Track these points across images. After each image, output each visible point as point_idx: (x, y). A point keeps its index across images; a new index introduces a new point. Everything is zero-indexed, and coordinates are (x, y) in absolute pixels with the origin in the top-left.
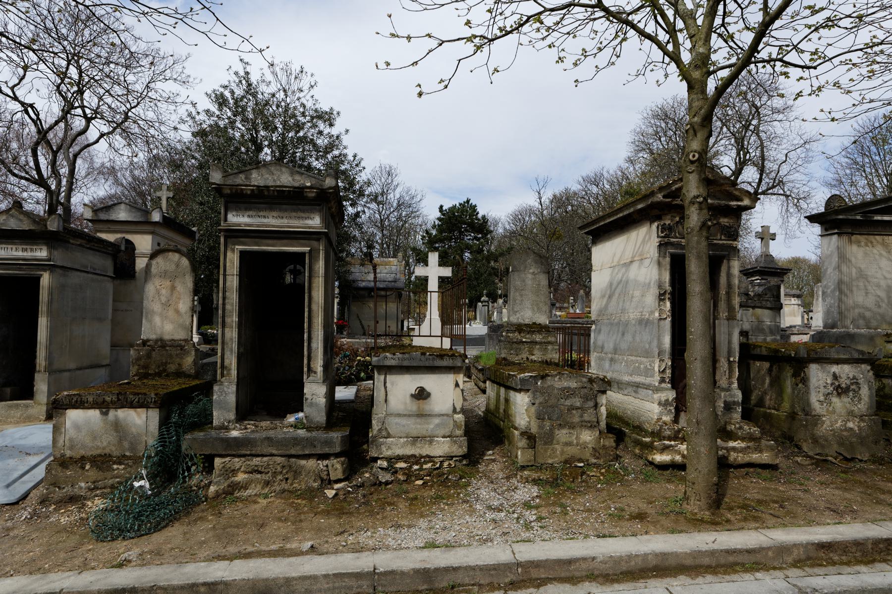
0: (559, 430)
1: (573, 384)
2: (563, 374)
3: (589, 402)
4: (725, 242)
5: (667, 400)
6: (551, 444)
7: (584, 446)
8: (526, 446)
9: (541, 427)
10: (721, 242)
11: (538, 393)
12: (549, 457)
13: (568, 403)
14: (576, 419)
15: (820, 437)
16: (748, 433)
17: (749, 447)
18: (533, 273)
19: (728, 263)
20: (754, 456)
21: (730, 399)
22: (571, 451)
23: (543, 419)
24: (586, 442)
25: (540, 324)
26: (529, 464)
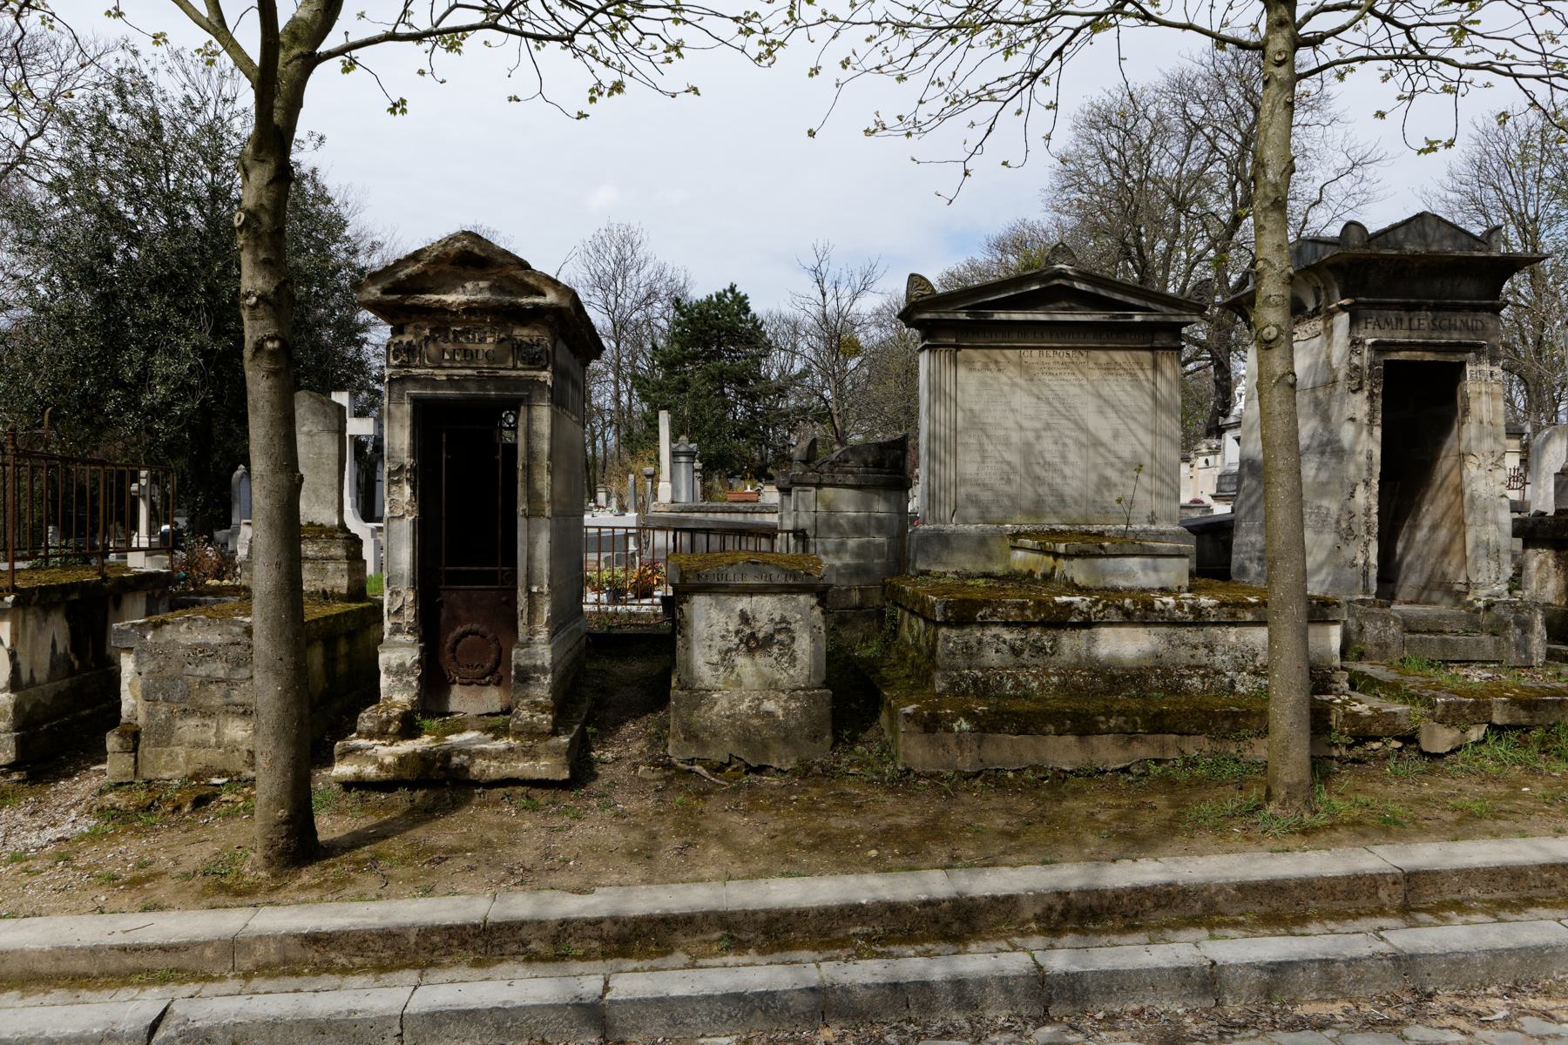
1: (214, 638)
3: (242, 670)
4: (522, 373)
5: (402, 665)
7: (234, 747)
8: (118, 749)
9: (150, 714)
10: (514, 373)
12: (165, 767)
13: (202, 671)
14: (217, 700)
15: (705, 729)
16: (527, 724)
17: (511, 750)
18: (309, 434)
19: (529, 411)
20: (521, 765)
21: (527, 662)
22: (203, 757)
23: (155, 700)
25: (321, 525)
26: (124, 780)
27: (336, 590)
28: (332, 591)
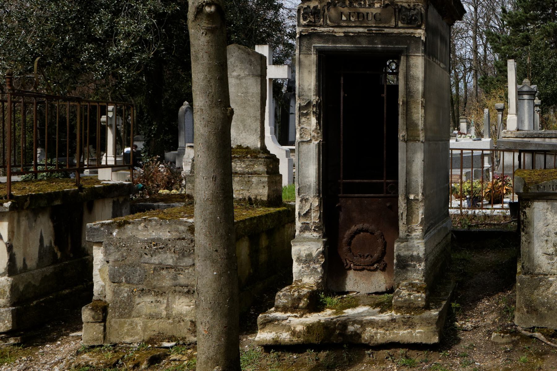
0: (139, 297)
1: (165, 234)
2: (150, 221)
3: (186, 259)
4: (402, 31)
5: (310, 255)
6: (130, 316)
7: (180, 318)
8: (91, 320)
9: (115, 293)
10: (396, 31)
11: (112, 248)
12: (127, 334)
13: (156, 260)
14: (167, 283)
15: (543, 304)
16: (405, 301)
17: (393, 320)
18: (238, 77)
19: (407, 61)
20: (401, 332)
21: (406, 253)
22: (157, 326)
23: (119, 283)
24: (181, 314)
25: (247, 148)
26: (96, 344)
27: (259, 198)
28: (256, 199)
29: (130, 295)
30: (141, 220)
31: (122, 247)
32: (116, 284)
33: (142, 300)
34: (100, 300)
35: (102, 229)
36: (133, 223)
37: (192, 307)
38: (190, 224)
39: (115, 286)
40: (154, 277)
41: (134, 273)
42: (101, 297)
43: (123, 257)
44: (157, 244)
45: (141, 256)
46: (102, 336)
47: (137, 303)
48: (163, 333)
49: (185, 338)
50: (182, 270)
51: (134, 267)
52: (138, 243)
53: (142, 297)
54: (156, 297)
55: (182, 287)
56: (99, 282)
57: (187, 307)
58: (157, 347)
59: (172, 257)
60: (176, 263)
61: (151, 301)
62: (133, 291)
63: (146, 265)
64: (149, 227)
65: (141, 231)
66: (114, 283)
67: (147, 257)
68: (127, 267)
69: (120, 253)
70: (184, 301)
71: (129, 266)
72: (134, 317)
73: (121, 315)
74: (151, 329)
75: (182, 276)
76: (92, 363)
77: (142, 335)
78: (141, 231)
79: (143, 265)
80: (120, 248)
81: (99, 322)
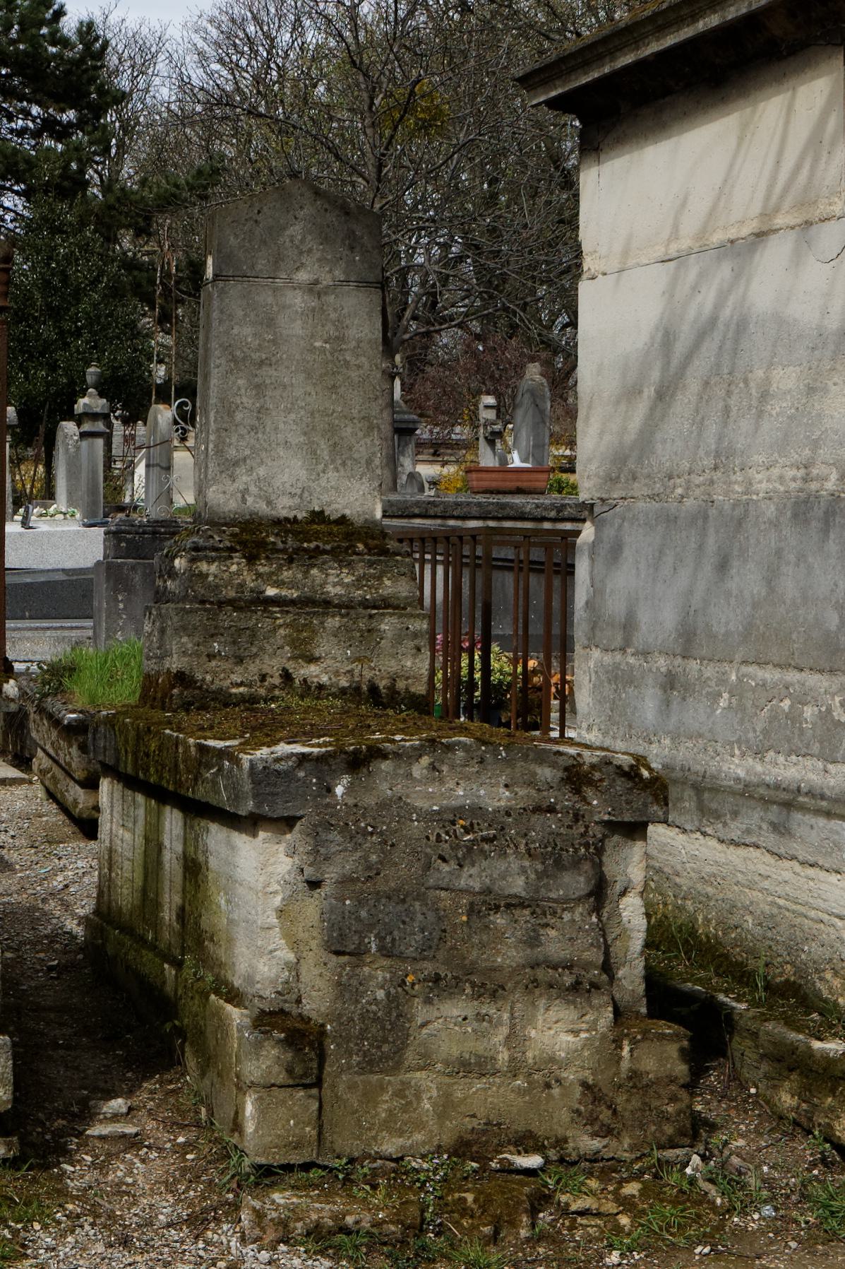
0: (428, 1001)
2: (449, 748)
3: (567, 878)
6: (397, 1067)
8: (282, 1078)
9: (345, 989)
11: (335, 836)
12: (390, 1125)
13: (472, 878)
14: (509, 955)
18: (312, 288)
23: (358, 954)
24: (552, 1060)
25: (343, 520)
26: (295, 1159)
27: (401, 685)
28: (392, 689)
29: (396, 997)
30: (422, 746)
31: (365, 833)
32: (345, 959)
33: (436, 1014)
34: (282, 1011)
35: (301, 774)
36: (397, 755)
37: (583, 1035)
38: (571, 762)
39: (343, 967)
40: (470, 937)
41: (404, 923)
42: (286, 1001)
43: (369, 868)
44: (472, 824)
45: (428, 867)
46: (314, 1133)
47: (420, 1021)
48: (499, 1124)
49: (565, 1140)
50: (554, 913)
51: (404, 901)
52: (413, 821)
53: (436, 1000)
54: (476, 1003)
55: (555, 968)
56: (277, 953)
57: (570, 1038)
58: (497, 1171)
59: (523, 871)
60: (537, 891)
61: (464, 1014)
62: (404, 982)
63: (443, 894)
64: (445, 768)
65: (420, 781)
66: (338, 953)
67: (445, 868)
68: (383, 900)
69: (359, 854)
70: (561, 1015)
71: (389, 898)
72: (410, 1069)
73: (370, 1063)
74: (462, 1109)
75: (553, 933)
76: (357, 1222)
77: (435, 1128)
78: (420, 781)
79: (431, 893)
80: (360, 839)
81: (306, 1086)
